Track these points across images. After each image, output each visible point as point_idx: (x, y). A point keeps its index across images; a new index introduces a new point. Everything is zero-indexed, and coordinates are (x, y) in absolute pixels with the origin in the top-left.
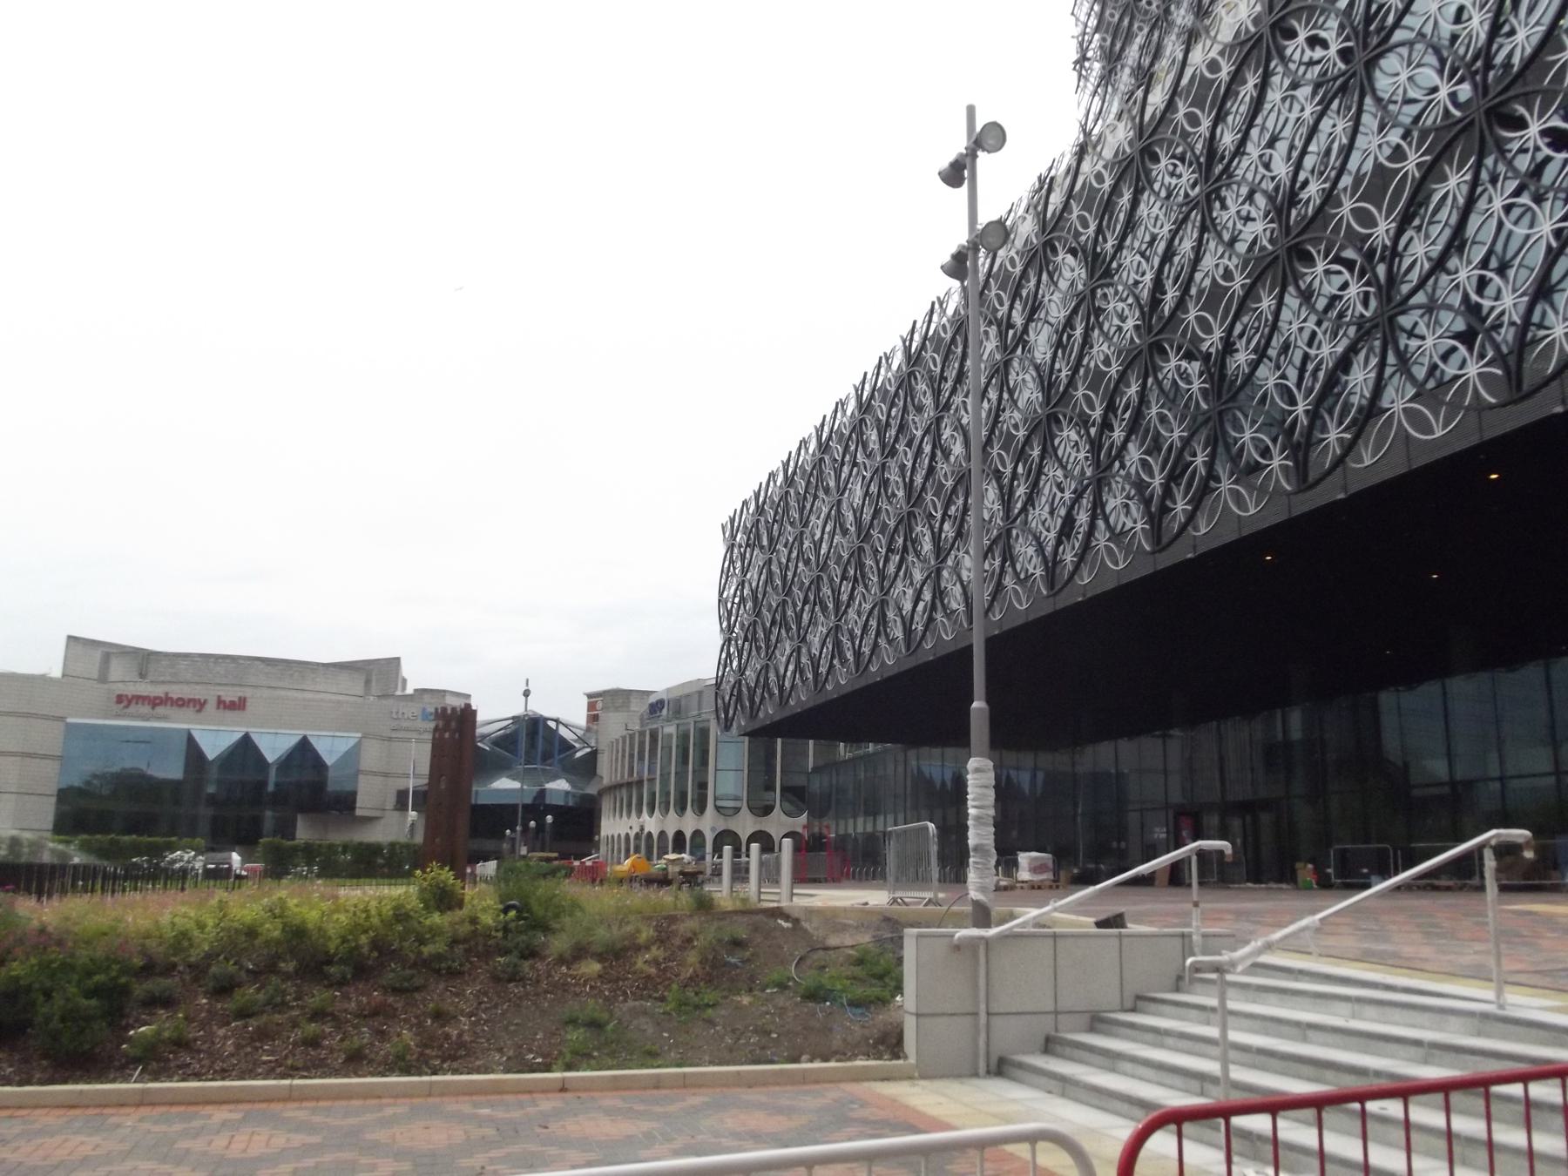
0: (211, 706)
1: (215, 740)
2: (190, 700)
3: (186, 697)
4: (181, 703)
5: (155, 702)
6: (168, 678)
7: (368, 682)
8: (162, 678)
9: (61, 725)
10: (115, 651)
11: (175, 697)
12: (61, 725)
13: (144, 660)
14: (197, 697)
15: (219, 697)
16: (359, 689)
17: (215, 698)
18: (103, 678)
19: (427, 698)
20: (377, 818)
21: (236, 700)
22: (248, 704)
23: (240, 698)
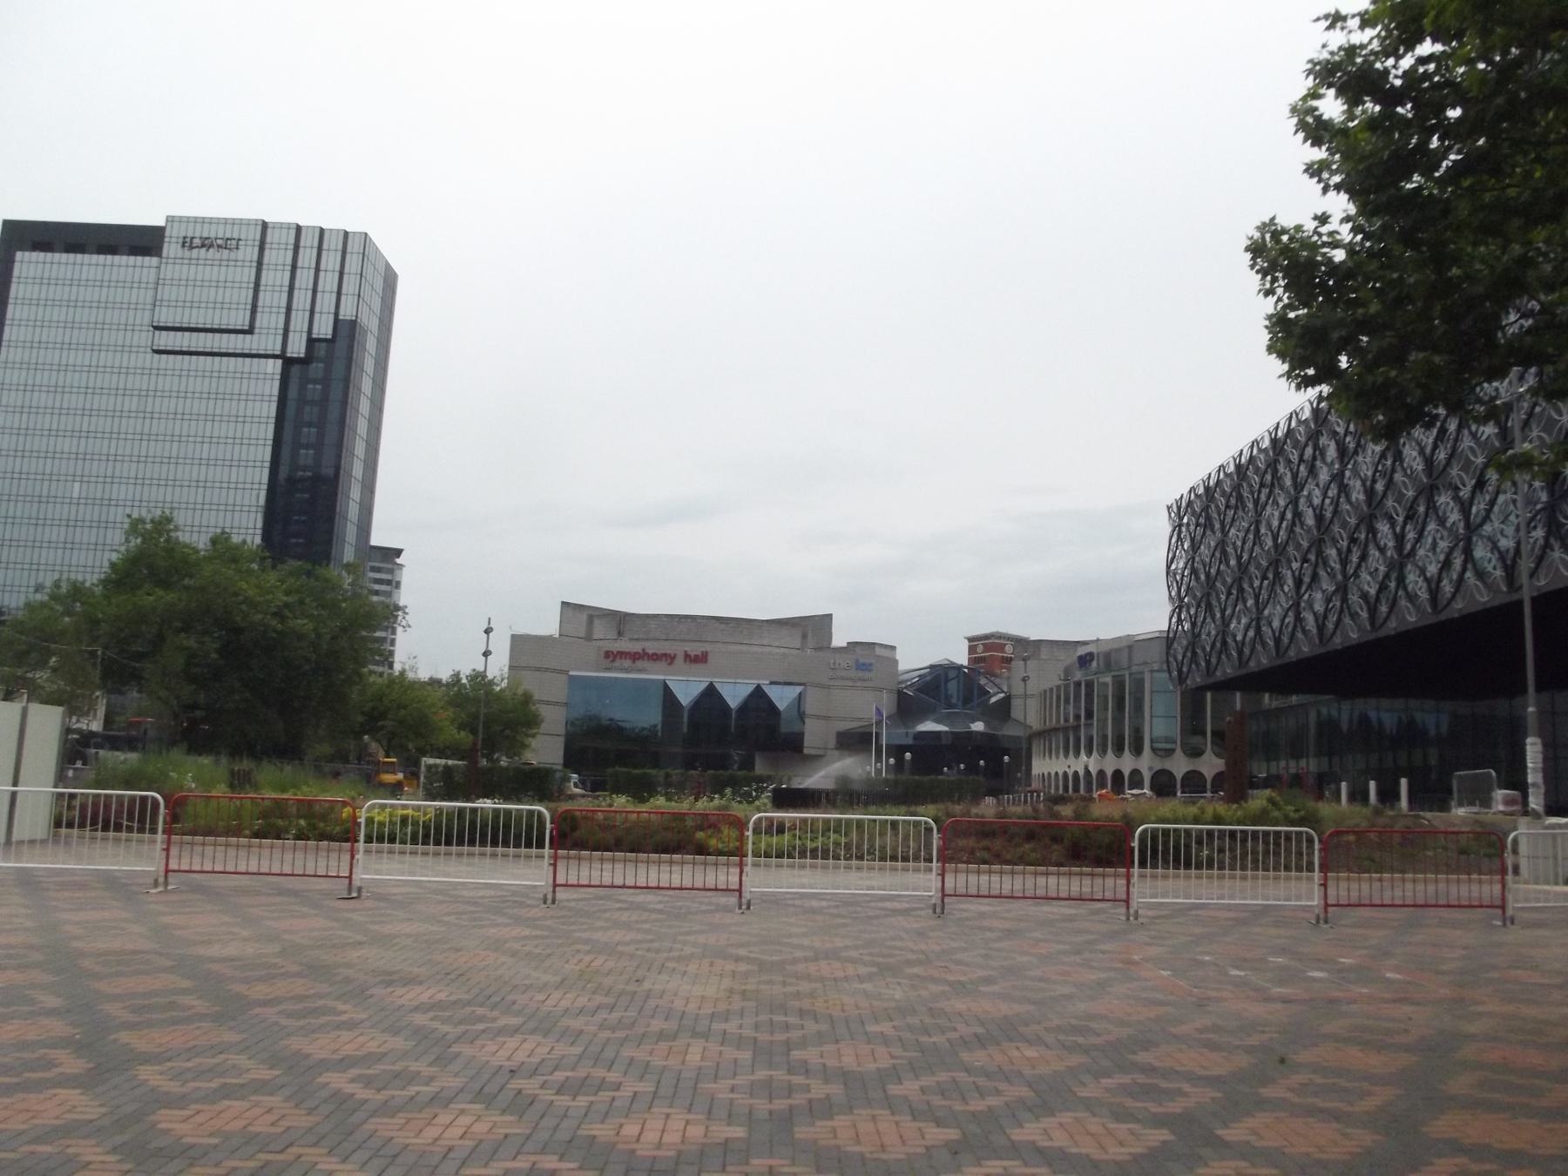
0: (680, 660)
1: (687, 689)
2: (665, 655)
3: (659, 652)
4: (655, 657)
5: (635, 657)
6: (641, 636)
7: (804, 636)
8: (636, 637)
9: (564, 677)
10: (597, 613)
11: (650, 652)
12: (564, 677)
13: (621, 621)
14: (668, 652)
15: (686, 652)
16: (797, 643)
17: (683, 653)
18: (589, 637)
19: (858, 650)
20: (821, 756)
21: (700, 654)
22: (709, 657)
23: (702, 652)
